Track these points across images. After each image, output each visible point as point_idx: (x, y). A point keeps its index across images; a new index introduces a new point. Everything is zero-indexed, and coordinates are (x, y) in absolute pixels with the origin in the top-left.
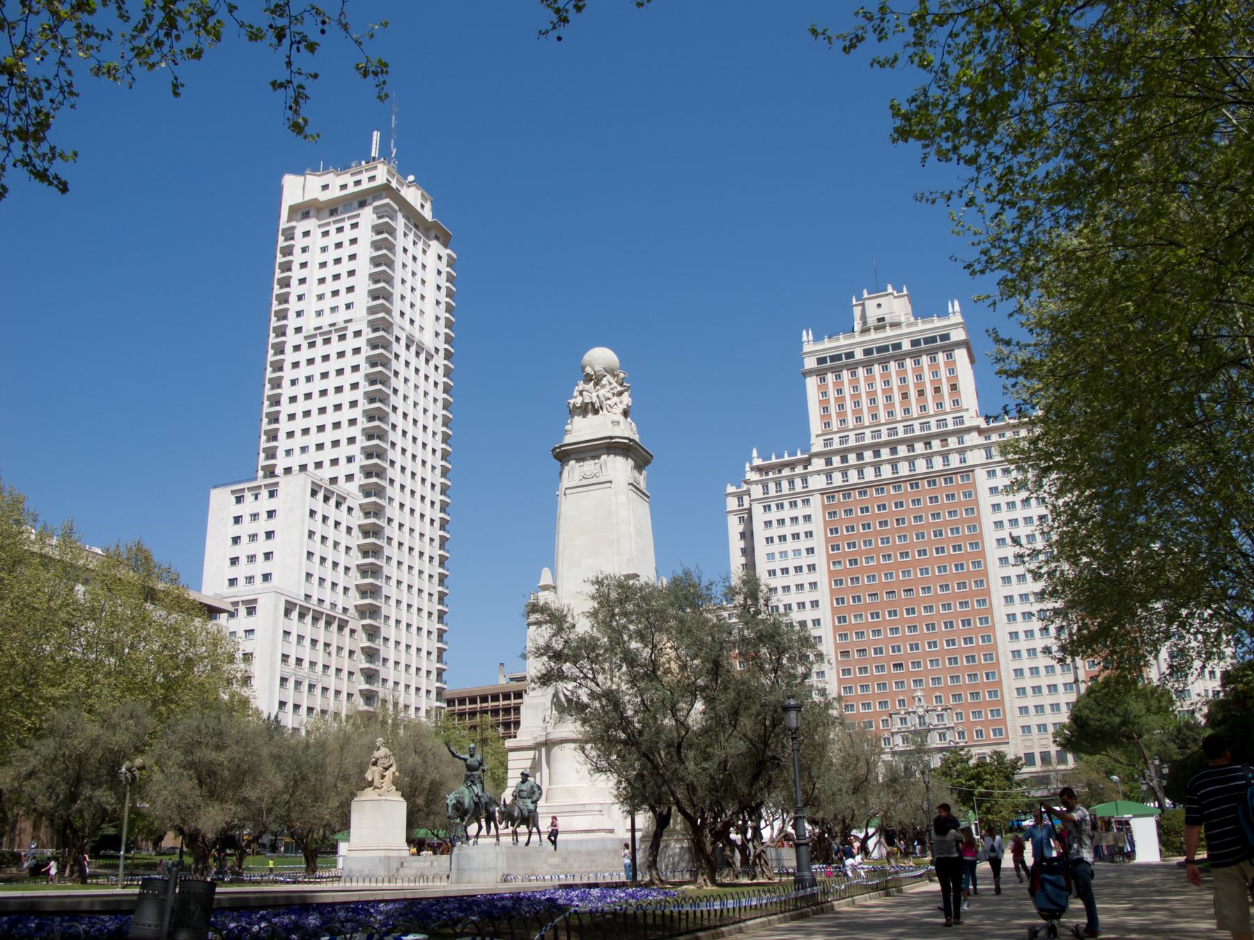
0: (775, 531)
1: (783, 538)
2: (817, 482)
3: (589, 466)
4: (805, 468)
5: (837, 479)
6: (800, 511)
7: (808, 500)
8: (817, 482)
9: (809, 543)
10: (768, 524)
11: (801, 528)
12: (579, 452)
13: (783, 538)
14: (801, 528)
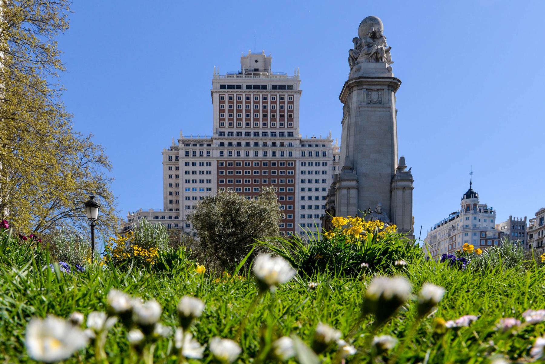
0: (191, 177)
1: (194, 181)
2: (215, 154)
3: (374, 96)
4: (209, 145)
5: (226, 154)
6: (205, 168)
7: (210, 163)
8: (215, 154)
9: (208, 185)
10: (187, 173)
11: (205, 177)
12: (370, 85)
13: (194, 181)
14: (205, 177)
